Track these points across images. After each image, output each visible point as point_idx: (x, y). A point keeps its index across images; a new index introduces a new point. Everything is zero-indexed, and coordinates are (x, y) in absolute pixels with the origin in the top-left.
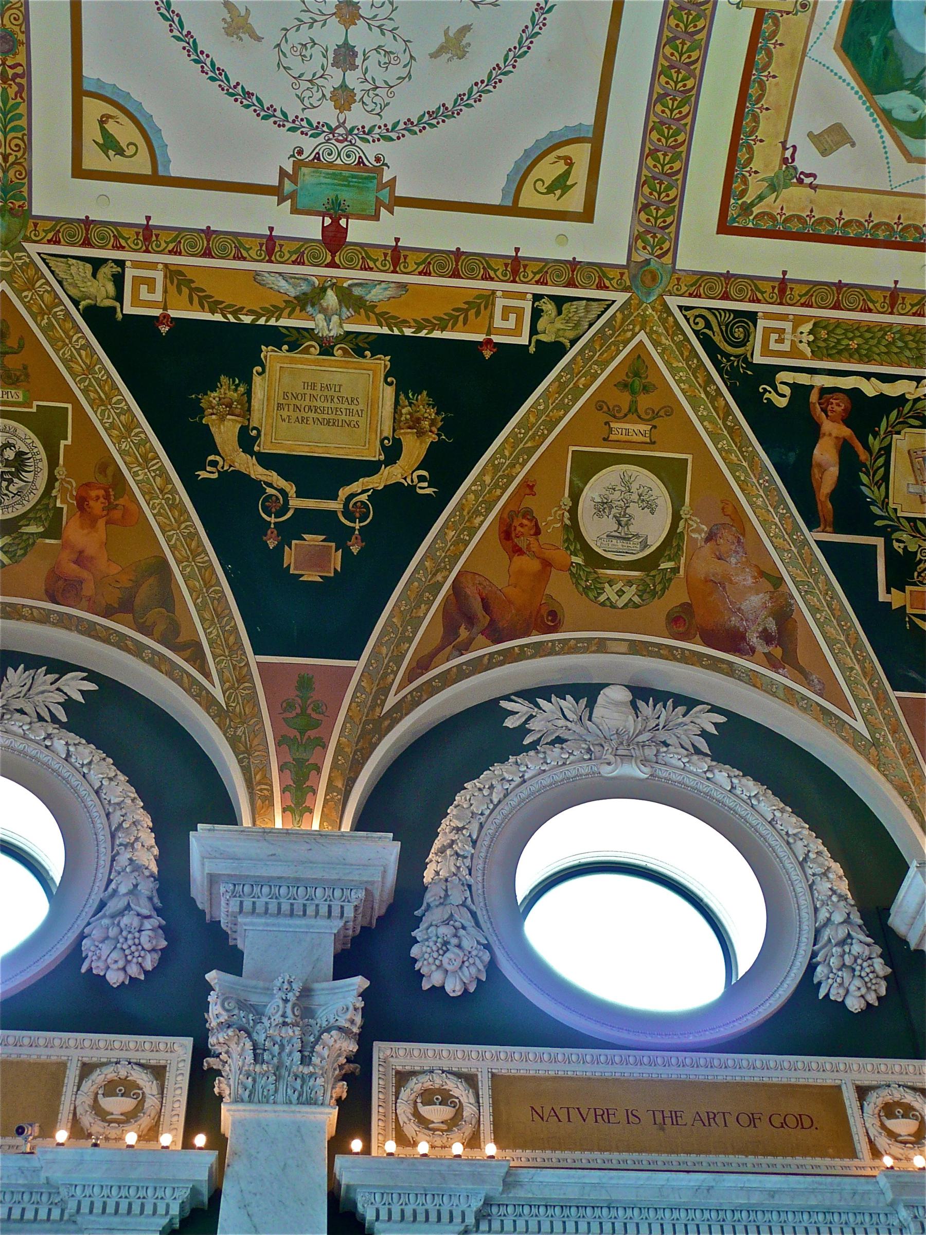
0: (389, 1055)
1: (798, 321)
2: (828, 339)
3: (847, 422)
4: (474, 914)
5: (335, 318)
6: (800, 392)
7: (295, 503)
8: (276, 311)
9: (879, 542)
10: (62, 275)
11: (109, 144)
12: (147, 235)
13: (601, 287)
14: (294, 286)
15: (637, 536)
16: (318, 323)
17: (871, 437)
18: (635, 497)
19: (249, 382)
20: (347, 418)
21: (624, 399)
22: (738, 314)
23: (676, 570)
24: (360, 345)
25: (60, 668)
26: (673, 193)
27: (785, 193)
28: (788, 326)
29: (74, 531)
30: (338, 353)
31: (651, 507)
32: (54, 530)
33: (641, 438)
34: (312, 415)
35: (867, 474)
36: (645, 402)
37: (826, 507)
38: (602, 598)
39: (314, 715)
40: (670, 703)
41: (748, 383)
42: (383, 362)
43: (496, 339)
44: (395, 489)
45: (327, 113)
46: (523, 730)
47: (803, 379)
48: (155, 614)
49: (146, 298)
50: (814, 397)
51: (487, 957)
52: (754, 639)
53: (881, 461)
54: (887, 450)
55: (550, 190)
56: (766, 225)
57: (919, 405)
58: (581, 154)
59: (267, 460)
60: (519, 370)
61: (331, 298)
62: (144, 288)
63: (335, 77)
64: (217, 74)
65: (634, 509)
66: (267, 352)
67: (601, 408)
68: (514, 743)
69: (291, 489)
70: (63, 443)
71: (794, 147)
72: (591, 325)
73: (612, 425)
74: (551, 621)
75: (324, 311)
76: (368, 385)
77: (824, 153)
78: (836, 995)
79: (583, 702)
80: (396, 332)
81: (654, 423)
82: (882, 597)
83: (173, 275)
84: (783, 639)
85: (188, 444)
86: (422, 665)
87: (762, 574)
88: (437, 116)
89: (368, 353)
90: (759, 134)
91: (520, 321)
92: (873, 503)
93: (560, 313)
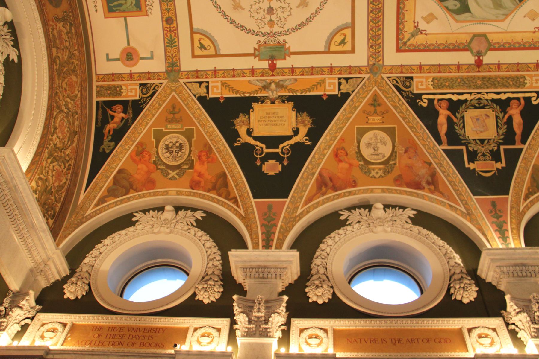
0: (297, 323)
1: (427, 78)
2: (438, 83)
3: (449, 109)
4: (328, 277)
5: (275, 92)
6: (431, 101)
7: (266, 151)
8: (256, 91)
9: (464, 148)
10: (190, 88)
11: (202, 47)
12: (215, 72)
13: (360, 73)
14: (261, 83)
15: (381, 154)
16: (269, 94)
17: (457, 114)
18: (379, 141)
19: (249, 114)
20: (281, 123)
21: (372, 109)
22: (406, 78)
23: (395, 164)
24: (284, 100)
25: (194, 210)
26: (380, 41)
27: (417, 37)
28: (424, 80)
29: (197, 166)
30: (276, 102)
31: (385, 144)
32: (192, 167)
33: (379, 121)
34: (269, 123)
35: (457, 126)
36: (379, 109)
37: (444, 138)
38: (371, 175)
39: (273, 217)
40: (397, 208)
41: (413, 100)
42: (291, 104)
43: (328, 93)
44: (298, 144)
45: (267, 29)
46: (347, 220)
47: (431, 97)
48: (223, 190)
49: (216, 91)
50: (436, 102)
51: (332, 291)
52: (424, 184)
53: (461, 121)
54: (463, 117)
55: (340, 44)
56: (412, 48)
57: (472, 102)
58: (348, 32)
59: (256, 138)
60: (335, 103)
61: (273, 86)
62: (215, 89)
63: (268, 17)
64: (232, 22)
65: (379, 145)
66: (254, 105)
67: (364, 113)
68: (344, 223)
69: (264, 146)
70: (193, 139)
71: (418, 22)
72: (358, 86)
73: (369, 118)
74: (354, 184)
75: (271, 90)
76: (287, 111)
77: (428, 23)
78: (459, 298)
79: (367, 210)
80: (295, 94)
81: (383, 115)
82: (467, 165)
83: (224, 84)
84: (433, 183)
85: (231, 135)
86: (309, 200)
87: (426, 162)
88: (301, 25)
89: (286, 102)
90: (406, 19)
91: (334, 87)
92: (460, 135)
93: (347, 83)
